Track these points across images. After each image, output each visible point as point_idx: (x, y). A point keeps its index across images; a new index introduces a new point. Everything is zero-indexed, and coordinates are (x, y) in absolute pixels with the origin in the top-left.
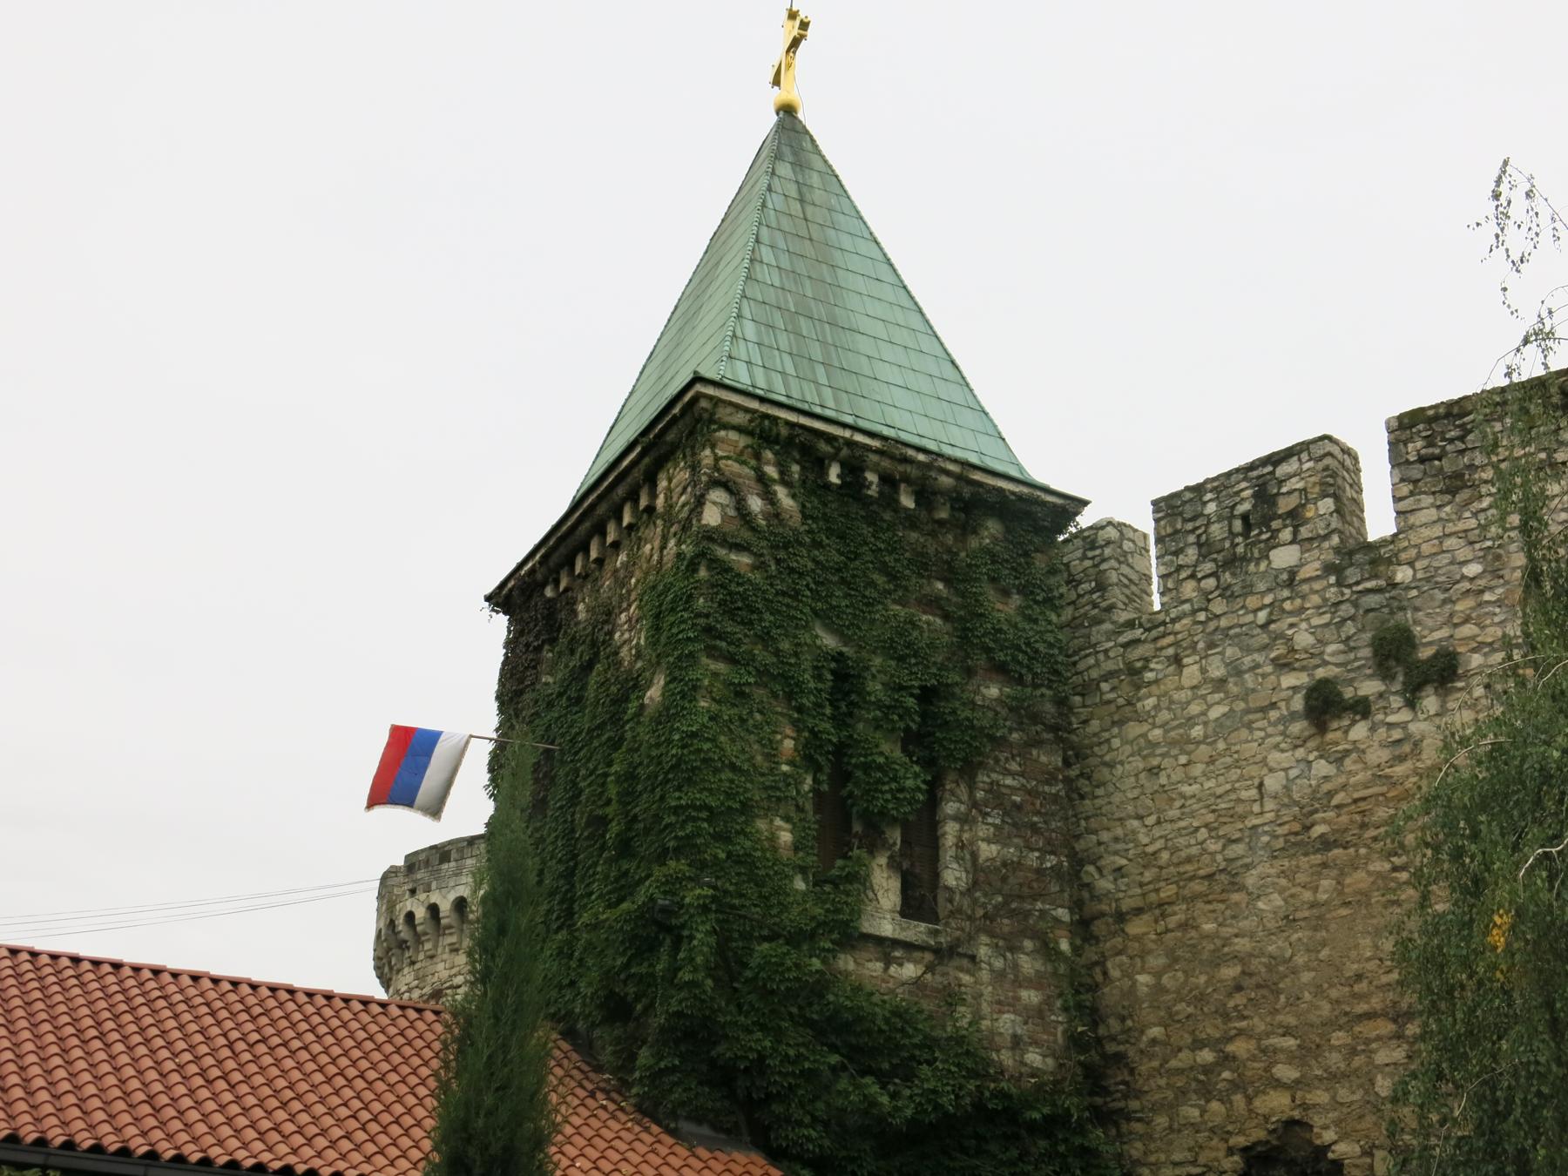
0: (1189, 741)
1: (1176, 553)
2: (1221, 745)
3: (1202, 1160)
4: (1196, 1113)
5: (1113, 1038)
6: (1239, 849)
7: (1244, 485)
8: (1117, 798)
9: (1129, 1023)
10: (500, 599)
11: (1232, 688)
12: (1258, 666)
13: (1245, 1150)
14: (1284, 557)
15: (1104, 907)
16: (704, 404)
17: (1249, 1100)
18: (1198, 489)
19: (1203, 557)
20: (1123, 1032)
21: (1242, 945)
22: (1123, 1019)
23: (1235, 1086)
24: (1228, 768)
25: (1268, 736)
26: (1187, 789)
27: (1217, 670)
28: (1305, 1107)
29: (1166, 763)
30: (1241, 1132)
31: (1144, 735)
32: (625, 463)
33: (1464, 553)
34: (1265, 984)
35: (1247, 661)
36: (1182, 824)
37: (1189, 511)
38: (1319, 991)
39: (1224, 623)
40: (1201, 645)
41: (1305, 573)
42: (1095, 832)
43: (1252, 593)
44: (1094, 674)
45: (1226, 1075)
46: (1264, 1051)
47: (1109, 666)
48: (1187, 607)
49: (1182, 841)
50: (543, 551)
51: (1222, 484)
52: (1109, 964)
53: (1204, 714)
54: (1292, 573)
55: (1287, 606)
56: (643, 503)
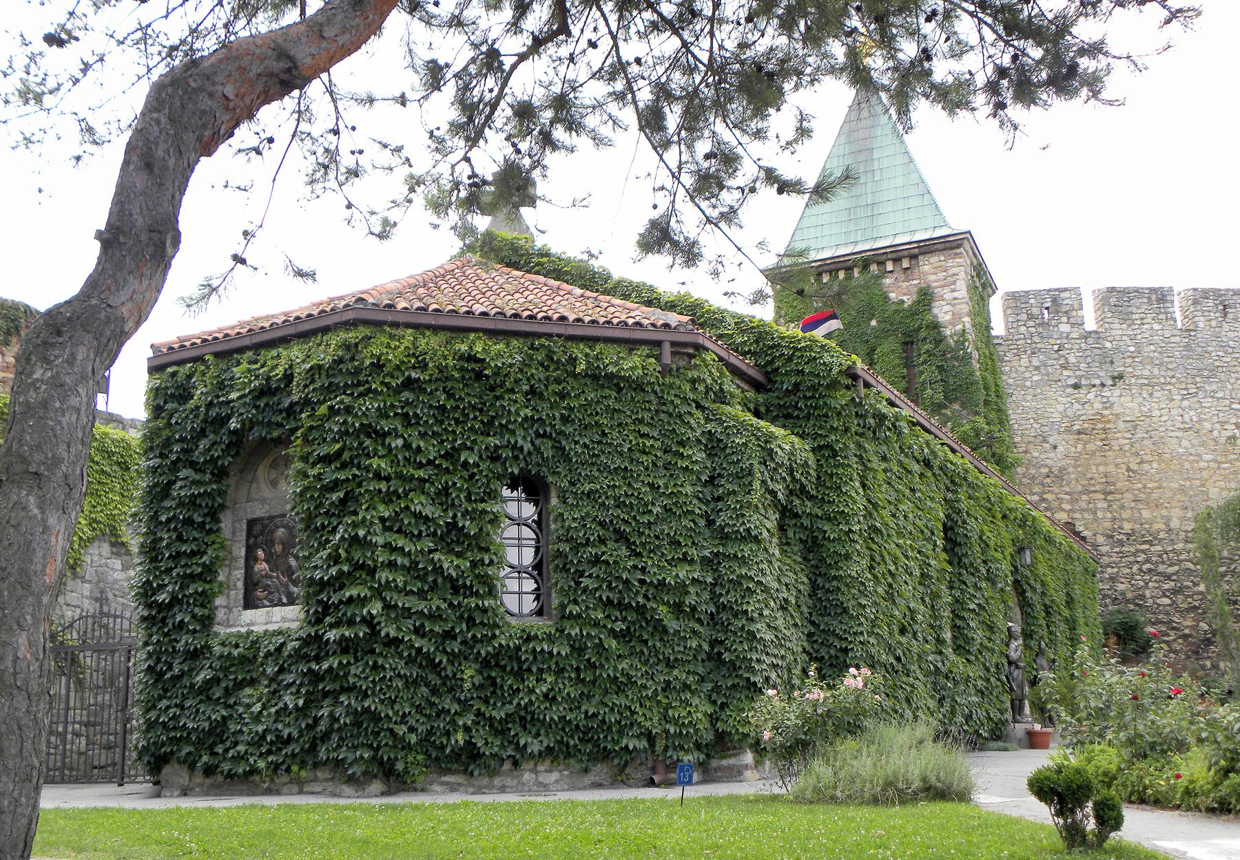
6: (1047, 429)
14: (1065, 328)
21: (1048, 462)
23: (1047, 509)
27: (1036, 363)
33: (1129, 342)
34: (1059, 476)
37: (1023, 300)
38: (1077, 481)
41: (1072, 336)
51: (1037, 293)
56: (906, 264)
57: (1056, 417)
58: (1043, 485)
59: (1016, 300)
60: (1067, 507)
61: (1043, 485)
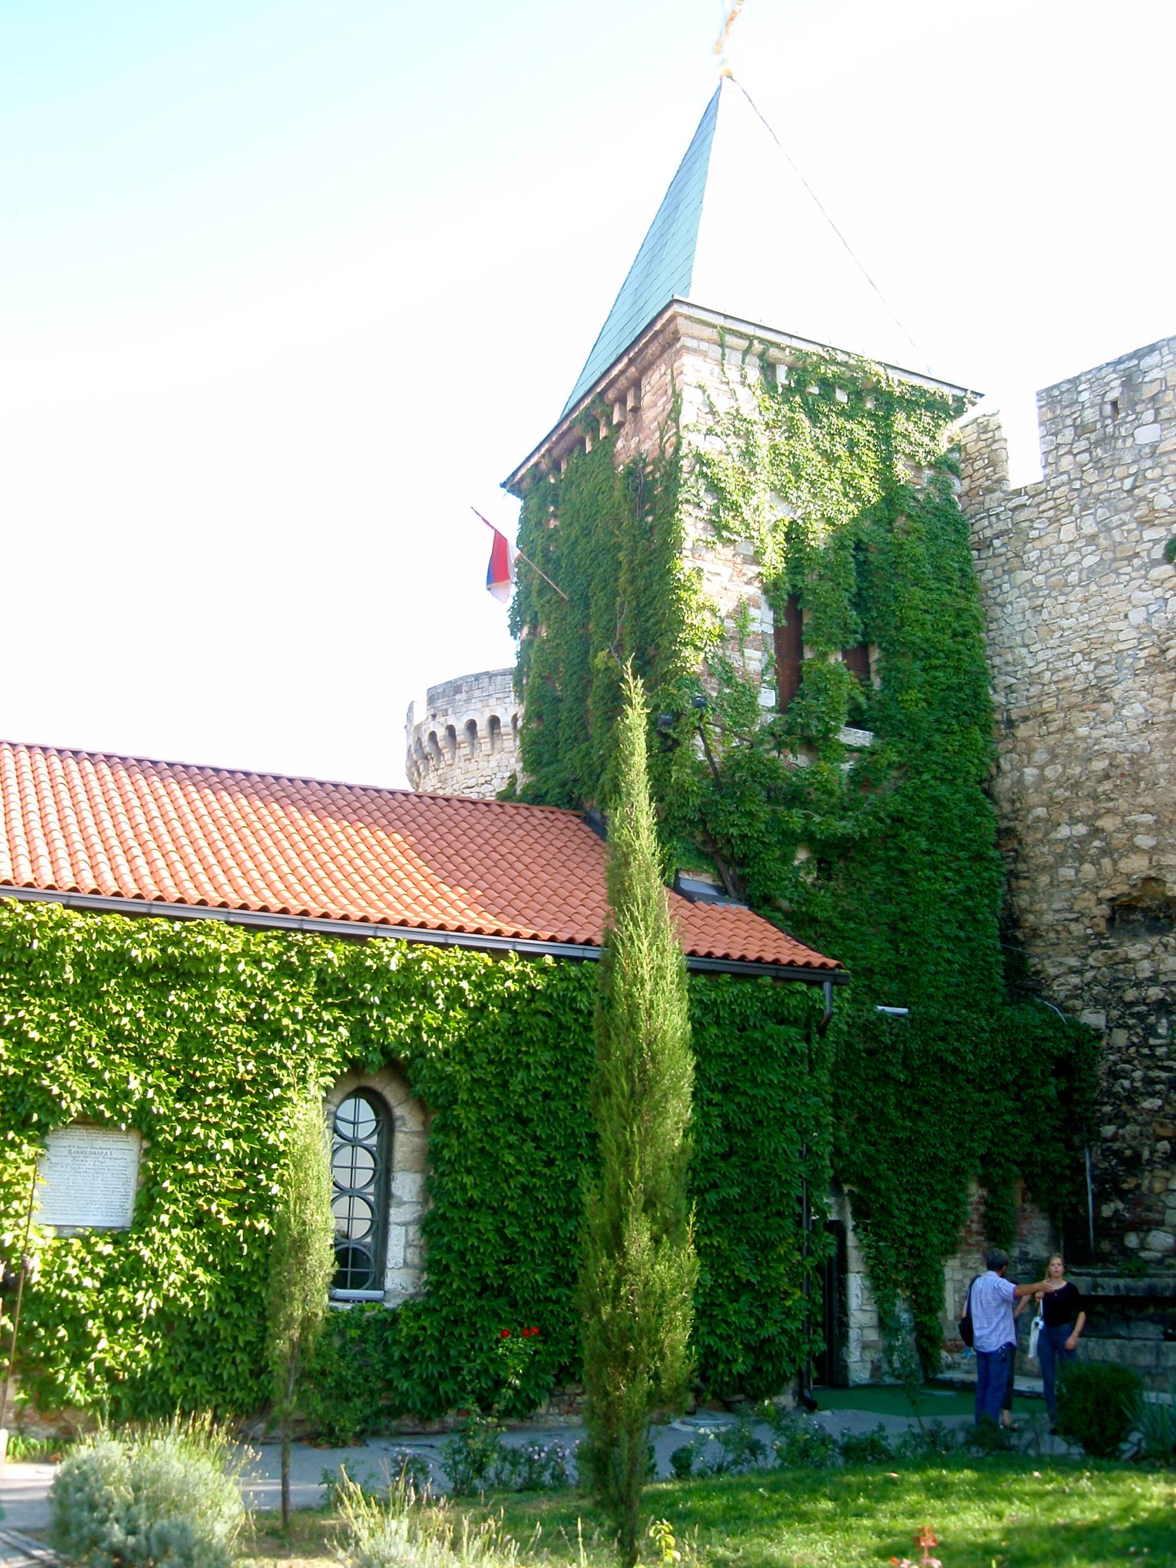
0: (1066, 585)
1: (1056, 434)
2: (1093, 588)
3: (1076, 908)
4: (1072, 872)
5: (1005, 817)
6: (1107, 669)
7: (1114, 376)
8: (1006, 632)
9: (1018, 805)
10: (512, 485)
11: (1103, 541)
12: (1124, 524)
13: (1112, 900)
15: (997, 717)
16: (680, 320)
17: (1115, 863)
18: (1075, 381)
19: (1078, 436)
20: (1014, 812)
21: (1110, 744)
22: (1013, 802)
23: (1103, 852)
24: (1099, 605)
25: (1132, 579)
26: (1065, 623)
28: (1160, 868)
29: (1048, 602)
30: (1108, 886)
31: (1030, 581)
32: (615, 372)
35: (1115, 520)
36: (1060, 650)
39: (1096, 489)
40: (1076, 508)
42: (990, 658)
43: (1119, 465)
44: (988, 533)
45: (1096, 843)
46: (1127, 825)
47: (1001, 526)
48: (1065, 477)
49: (1060, 664)
50: (547, 446)
51: (1095, 376)
52: (1002, 761)
53: (1079, 563)
54: (1154, 447)
55: (1149, 474)
56: (630, 404)
57: (1129, 635)
58: (1095, 798)
59: (1056, 401)
60: (1145, 841)
61: (1095, 798)
